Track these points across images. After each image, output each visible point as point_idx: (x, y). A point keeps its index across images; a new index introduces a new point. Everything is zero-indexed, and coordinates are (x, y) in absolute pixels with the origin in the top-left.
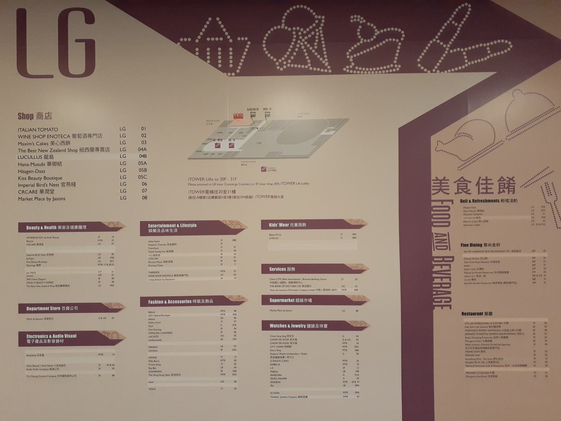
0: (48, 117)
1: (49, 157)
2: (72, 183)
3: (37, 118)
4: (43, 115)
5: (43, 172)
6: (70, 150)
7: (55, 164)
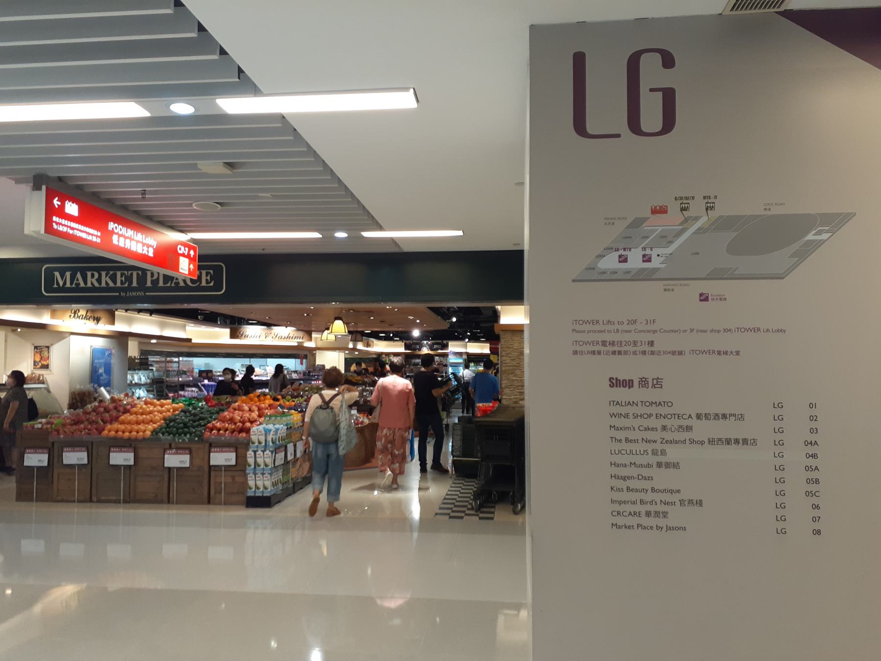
0: (657, 384)
1: (659, 453)
2: (697, 501)
3: (639, 386)
4: (648, 381)
5: (650, 478)
6: (692, 442)
7: (668, 465)
